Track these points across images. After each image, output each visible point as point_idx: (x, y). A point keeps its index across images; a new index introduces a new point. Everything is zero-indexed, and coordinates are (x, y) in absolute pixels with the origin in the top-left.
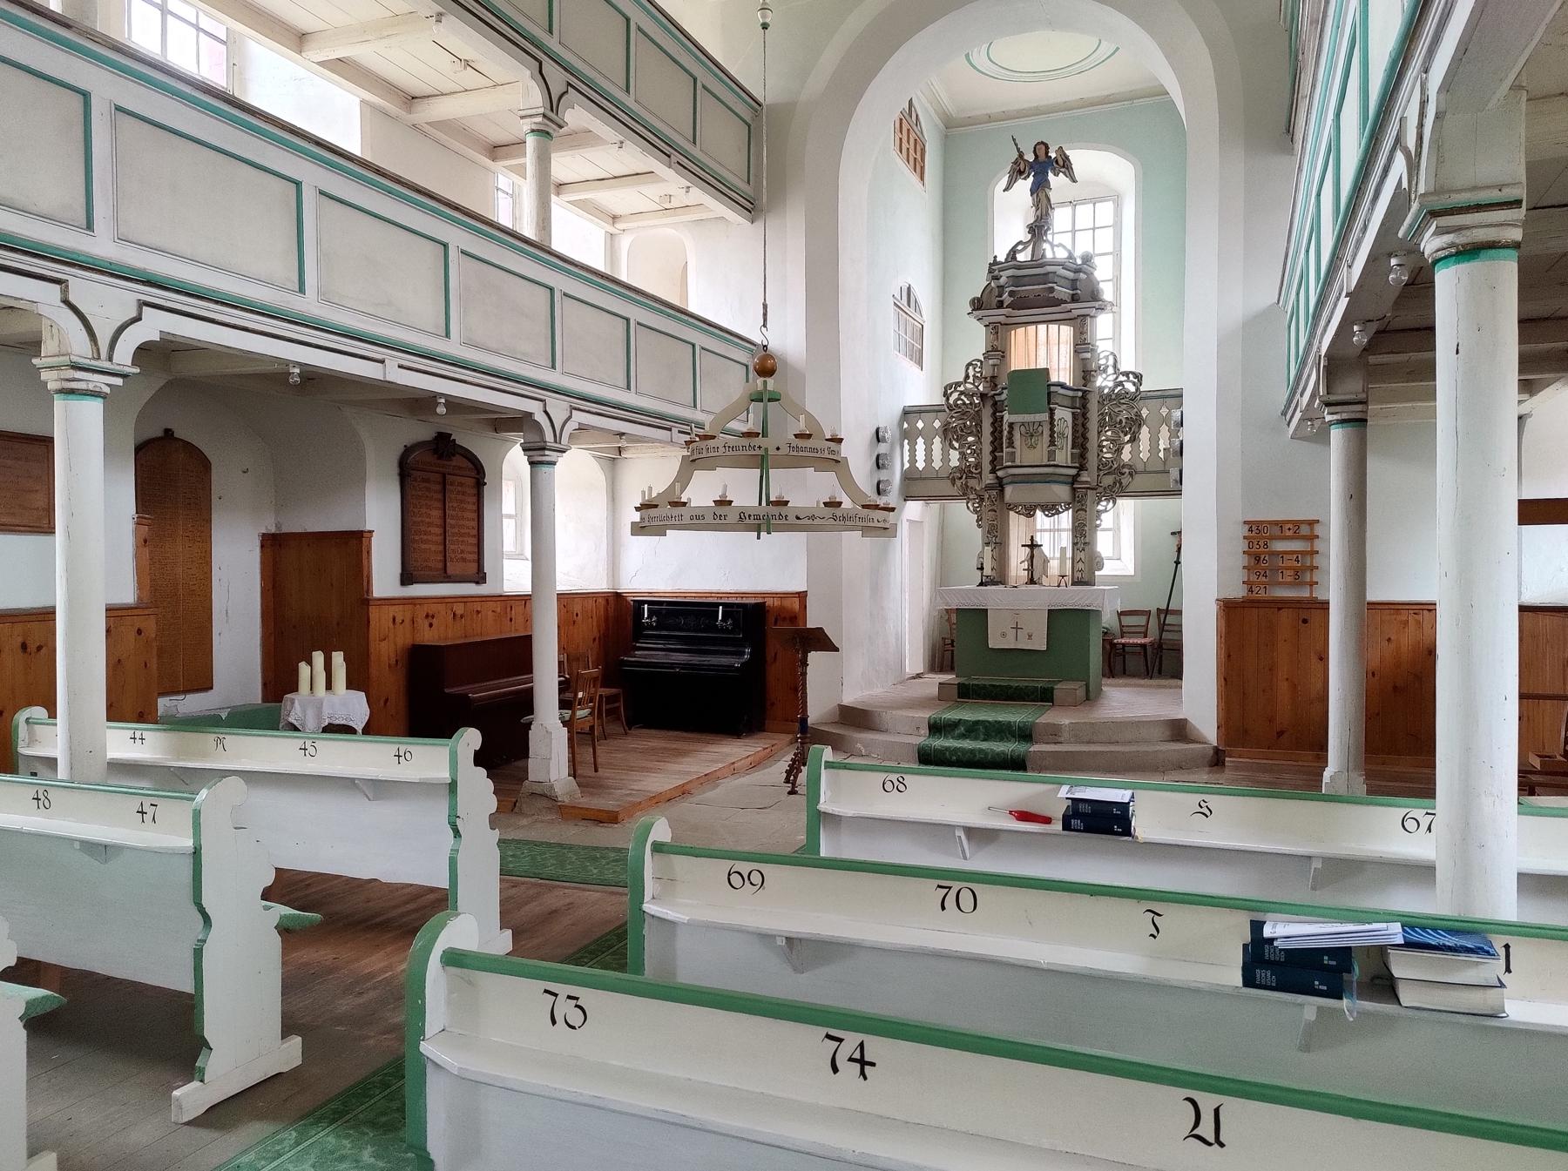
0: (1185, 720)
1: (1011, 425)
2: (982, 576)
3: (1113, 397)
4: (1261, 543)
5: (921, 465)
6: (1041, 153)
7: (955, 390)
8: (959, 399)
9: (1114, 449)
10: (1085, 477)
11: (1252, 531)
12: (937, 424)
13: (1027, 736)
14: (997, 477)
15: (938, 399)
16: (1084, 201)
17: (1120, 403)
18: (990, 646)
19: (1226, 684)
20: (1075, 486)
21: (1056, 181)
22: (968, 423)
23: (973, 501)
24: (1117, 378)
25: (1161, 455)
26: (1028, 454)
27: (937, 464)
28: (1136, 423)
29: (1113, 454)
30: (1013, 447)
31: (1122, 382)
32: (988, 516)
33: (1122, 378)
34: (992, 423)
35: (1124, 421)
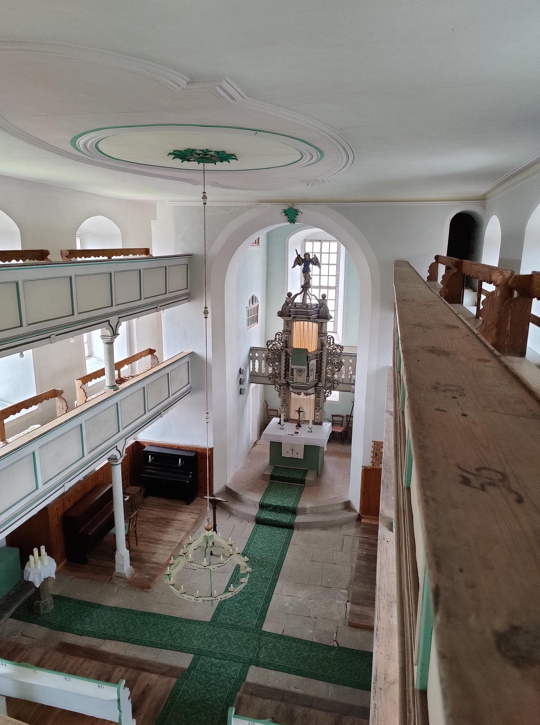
0: (350, 501)
1: (292, 369)
4: (378, 449)
5: (257, 370)
7: (271, 343)
8: (272, 347)
10: (320, 385)
11: (375, 445)
12: (263, 355)
13: (294, 513)
15: (264, 346)
16: (326, 241)
17: (334, 356)
18: (282, 456)
19: (363, 495)
21: (314, 269)
24: (334, 347)
25: (349, 377)
26: (299, 379)
28: (340, 364)
31: (336, 348)
32: (282, 395)
33: (335, 347)
35: (336, 363)
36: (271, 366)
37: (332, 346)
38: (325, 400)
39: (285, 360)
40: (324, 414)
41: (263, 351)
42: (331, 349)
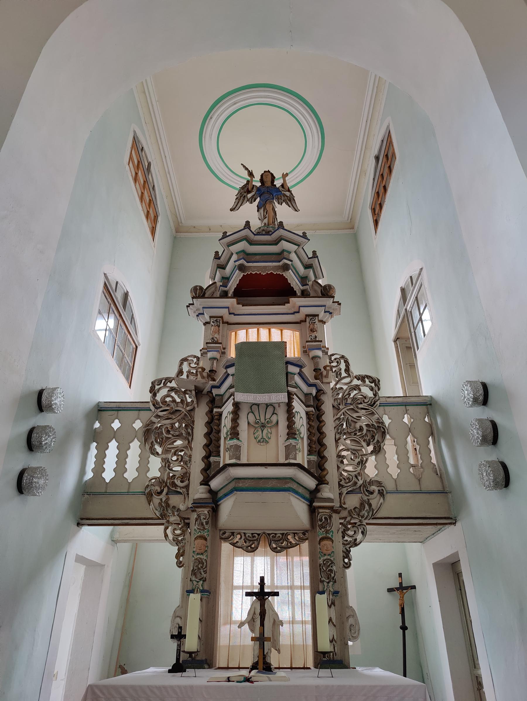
2: (179, 651)
3: (349, 401)
5: (108, 475)
6: (268, 179)
8: (168, 396)
9: (357, 460)
12: (138, 425)
14: (210, 491)
17: (357, 407)
20: (316, 504)
22: (177, 425)
23: (175, 526)
24: (351, 381)
27: (131, 474)
30: (238, 439)
33: (356, 382)
34: (207, 422)
35: (365, 428)
36: (157, 453)
37: (347, 380)
38: (346, 560)
40: (351, 621)
41: (136, 412)
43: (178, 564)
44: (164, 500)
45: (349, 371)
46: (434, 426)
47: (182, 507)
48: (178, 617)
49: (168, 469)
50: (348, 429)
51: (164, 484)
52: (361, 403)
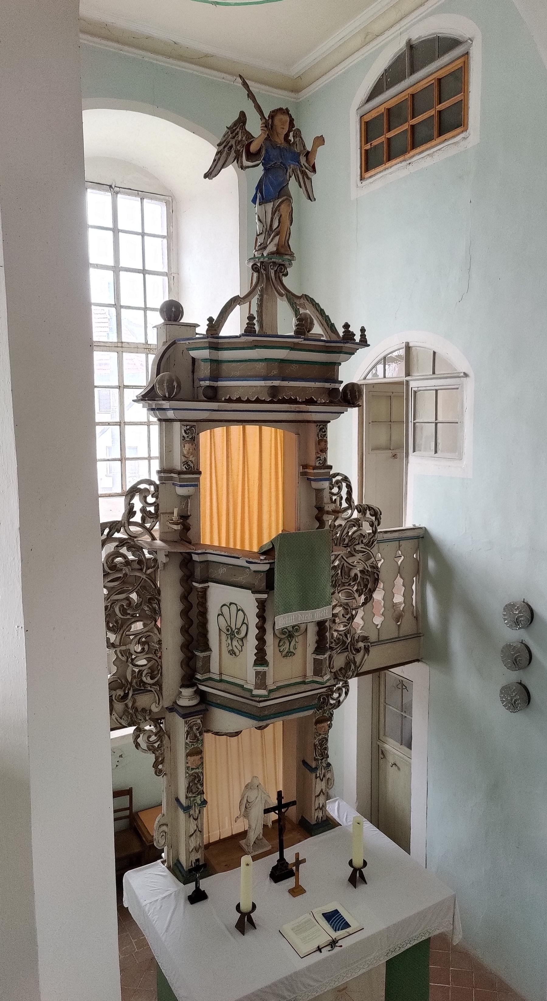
9: (348, 617)
29: (345, 626)
35: (359, 575)
39: (185, 598)
42: (343, 523)
43: (158, 774)
44: (130, 705)
45: (351, 499)
46: (421, 563)
47: (155, 709)
48: (163, 825)
49: (130, 665)
50: (342, 579)
51: (129, 686)
52: (359, 544)
